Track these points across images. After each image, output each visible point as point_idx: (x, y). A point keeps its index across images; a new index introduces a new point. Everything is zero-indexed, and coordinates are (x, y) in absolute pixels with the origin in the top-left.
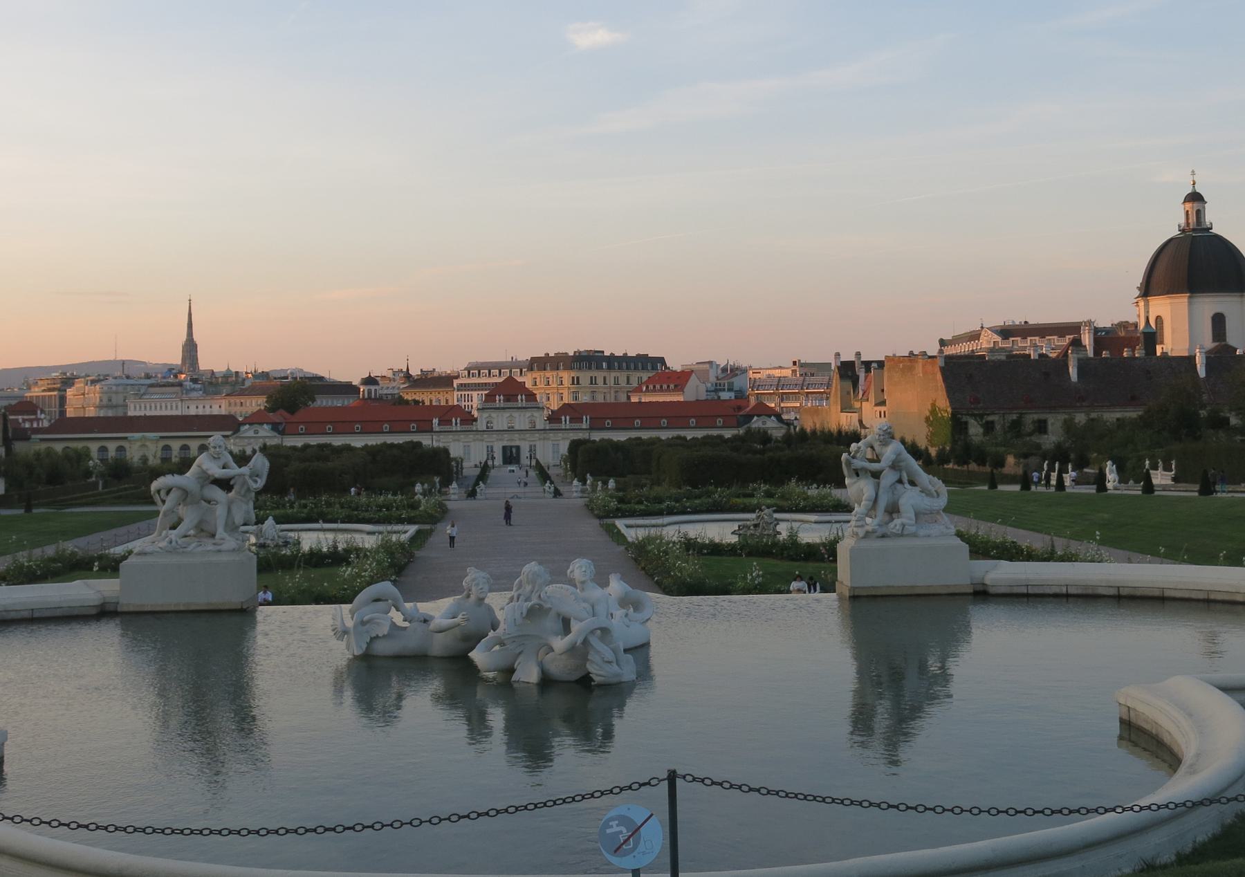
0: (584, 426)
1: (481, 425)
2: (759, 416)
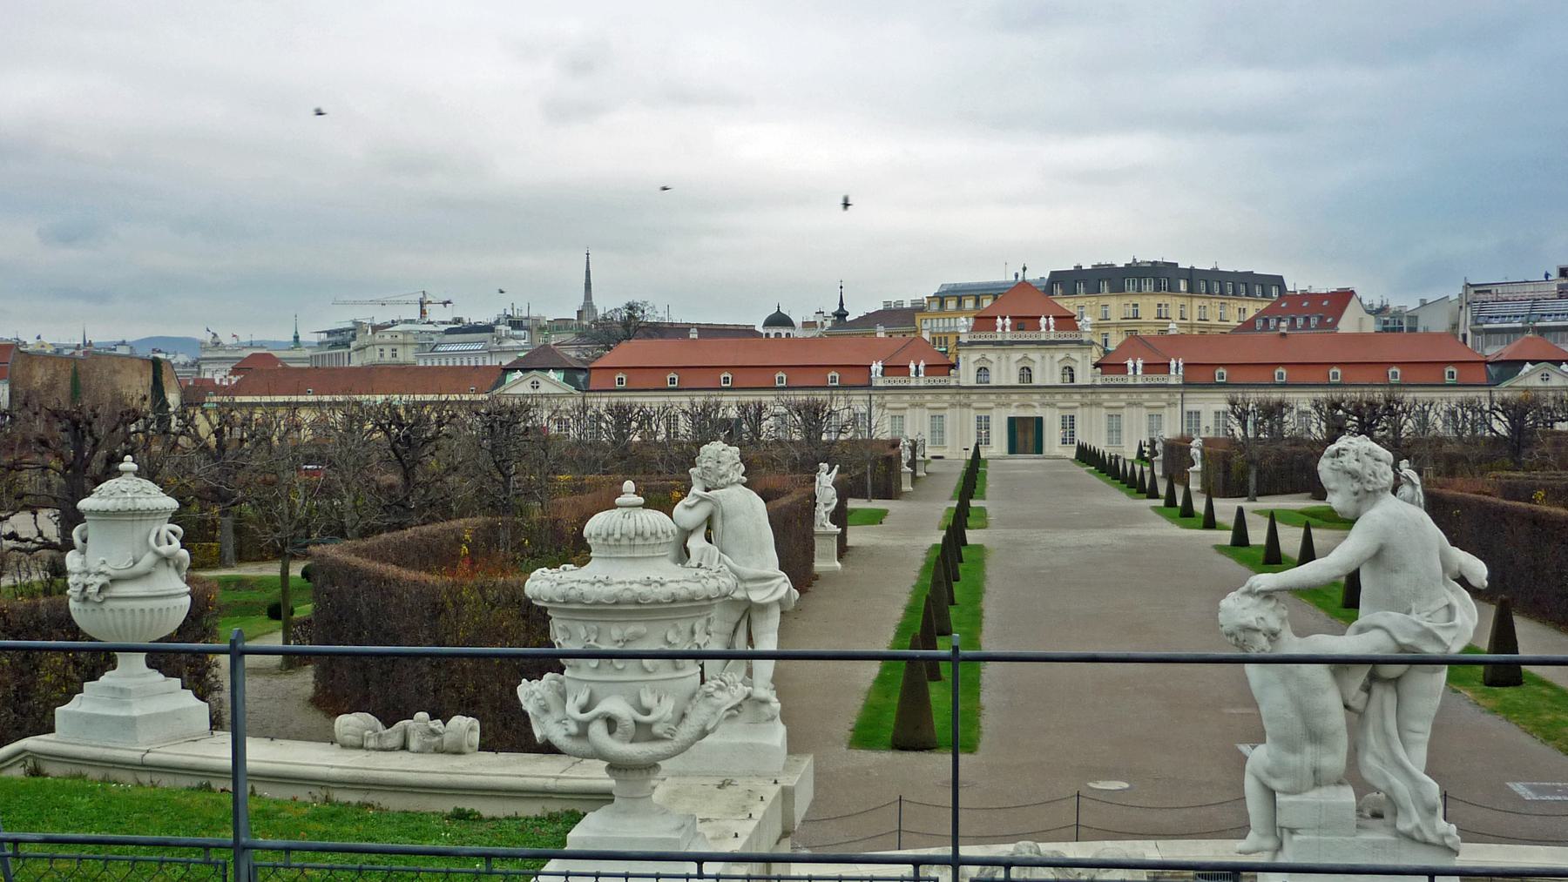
0: (1173, 381)
1: (966, 374)
2: (1533, 362)
